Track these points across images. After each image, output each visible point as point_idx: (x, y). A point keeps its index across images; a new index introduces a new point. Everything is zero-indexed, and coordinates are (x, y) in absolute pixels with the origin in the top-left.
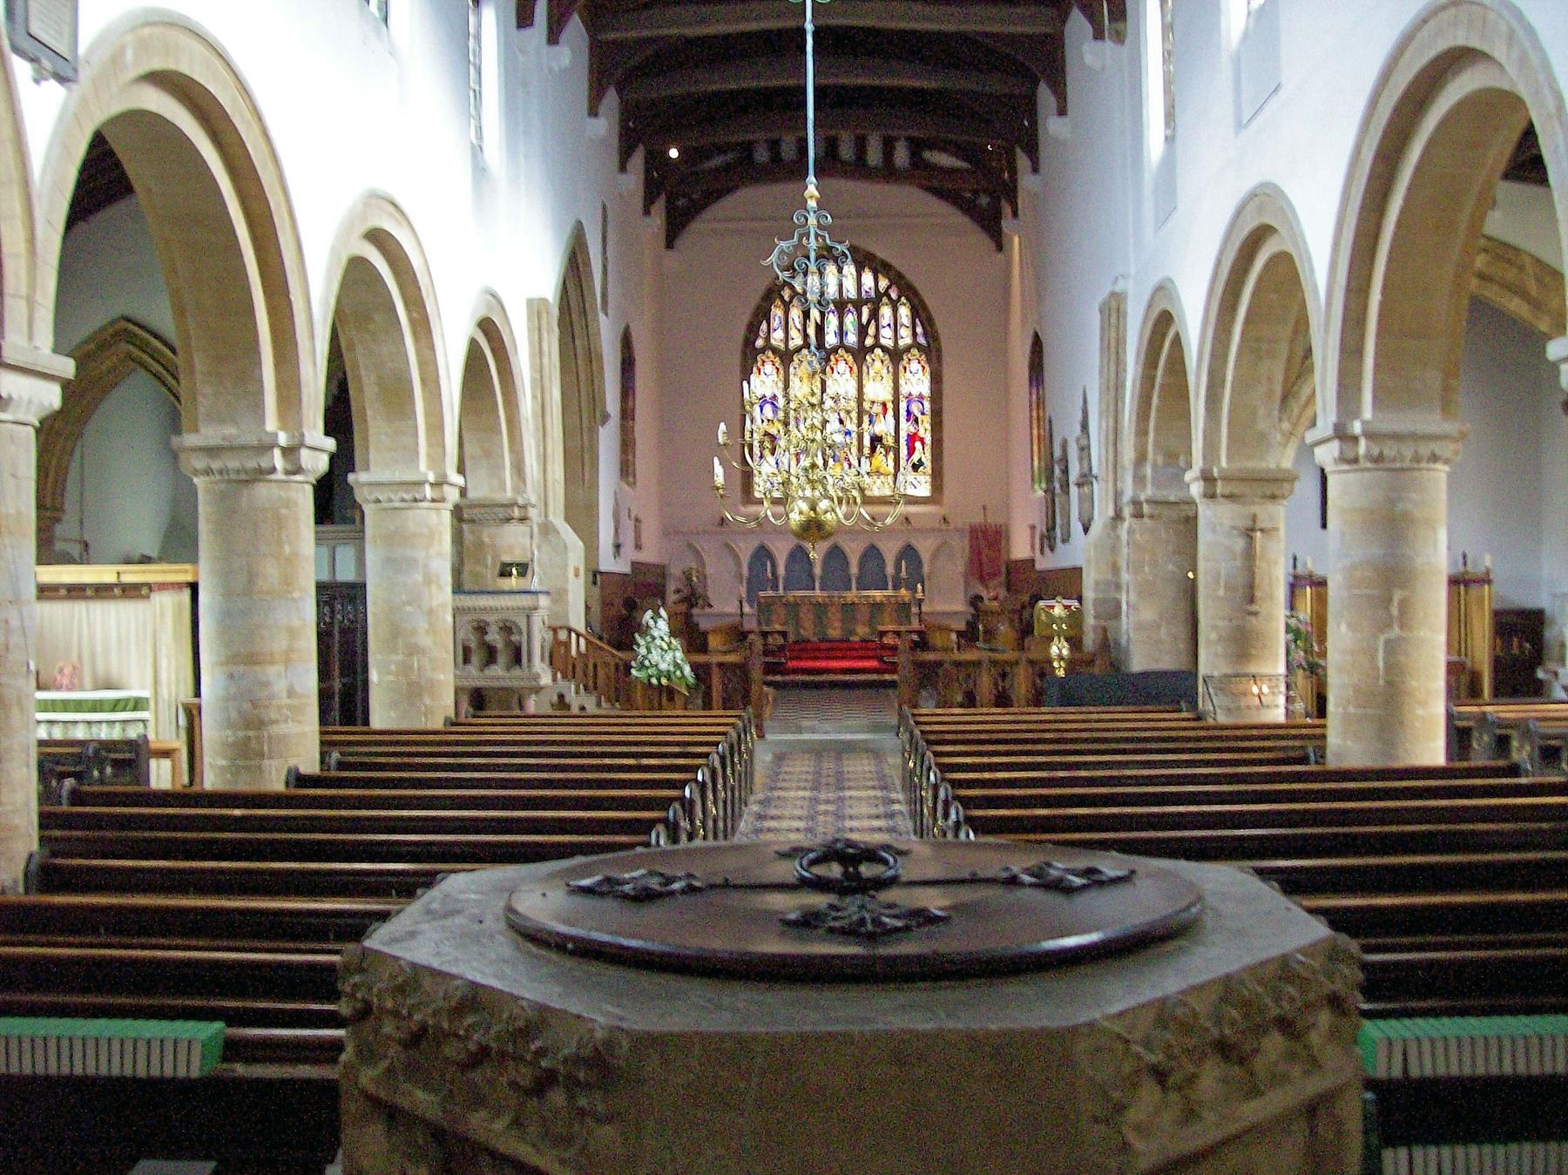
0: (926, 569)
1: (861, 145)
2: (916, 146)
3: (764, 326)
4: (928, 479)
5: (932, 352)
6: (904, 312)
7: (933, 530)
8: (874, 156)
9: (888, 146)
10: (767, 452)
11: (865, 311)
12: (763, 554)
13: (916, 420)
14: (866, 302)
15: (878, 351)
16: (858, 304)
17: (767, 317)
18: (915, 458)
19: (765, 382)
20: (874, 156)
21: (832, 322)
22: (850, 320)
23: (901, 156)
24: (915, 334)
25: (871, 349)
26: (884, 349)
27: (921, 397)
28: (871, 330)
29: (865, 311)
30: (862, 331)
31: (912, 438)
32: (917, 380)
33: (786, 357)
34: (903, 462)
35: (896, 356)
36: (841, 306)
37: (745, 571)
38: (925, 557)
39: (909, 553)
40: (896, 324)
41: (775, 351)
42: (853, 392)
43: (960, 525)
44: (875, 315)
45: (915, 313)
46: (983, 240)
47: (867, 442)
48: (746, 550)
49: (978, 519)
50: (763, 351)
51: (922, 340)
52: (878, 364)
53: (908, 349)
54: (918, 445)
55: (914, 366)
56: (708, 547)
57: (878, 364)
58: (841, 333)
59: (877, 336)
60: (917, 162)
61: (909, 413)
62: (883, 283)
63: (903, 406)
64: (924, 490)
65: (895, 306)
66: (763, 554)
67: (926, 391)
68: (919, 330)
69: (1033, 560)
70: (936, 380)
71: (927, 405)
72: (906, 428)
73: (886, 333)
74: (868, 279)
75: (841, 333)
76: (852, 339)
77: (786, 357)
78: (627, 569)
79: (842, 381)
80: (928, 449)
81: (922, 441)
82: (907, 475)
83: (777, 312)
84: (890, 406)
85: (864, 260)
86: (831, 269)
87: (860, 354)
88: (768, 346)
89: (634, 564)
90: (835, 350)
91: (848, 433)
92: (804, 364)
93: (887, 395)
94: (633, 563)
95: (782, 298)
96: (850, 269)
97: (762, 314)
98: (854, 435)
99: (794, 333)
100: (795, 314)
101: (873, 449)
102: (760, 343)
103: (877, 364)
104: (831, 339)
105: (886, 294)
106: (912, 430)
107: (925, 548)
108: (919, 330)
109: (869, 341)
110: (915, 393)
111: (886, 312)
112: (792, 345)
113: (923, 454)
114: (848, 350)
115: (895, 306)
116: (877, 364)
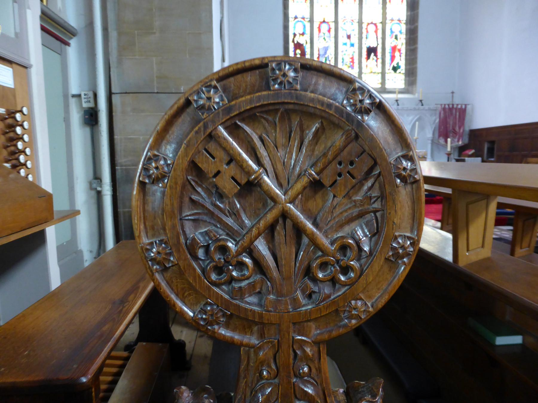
4: (403, 77)
7: (415, 109)
13: (396, 38)
18: (394, 64)
31: (394, 49)
43: (432, 106)
49: (447, 101)
54: (397, 54)
61: (392, 32)
67: (404, 18)
72: (390, 43)
80: (403, 56)
81: (399, 50)
82: (390, 74)
84: (380, 26)
91: (352, 45)
101: (368, 57)
110: (396, 18)
113: (401, 60)
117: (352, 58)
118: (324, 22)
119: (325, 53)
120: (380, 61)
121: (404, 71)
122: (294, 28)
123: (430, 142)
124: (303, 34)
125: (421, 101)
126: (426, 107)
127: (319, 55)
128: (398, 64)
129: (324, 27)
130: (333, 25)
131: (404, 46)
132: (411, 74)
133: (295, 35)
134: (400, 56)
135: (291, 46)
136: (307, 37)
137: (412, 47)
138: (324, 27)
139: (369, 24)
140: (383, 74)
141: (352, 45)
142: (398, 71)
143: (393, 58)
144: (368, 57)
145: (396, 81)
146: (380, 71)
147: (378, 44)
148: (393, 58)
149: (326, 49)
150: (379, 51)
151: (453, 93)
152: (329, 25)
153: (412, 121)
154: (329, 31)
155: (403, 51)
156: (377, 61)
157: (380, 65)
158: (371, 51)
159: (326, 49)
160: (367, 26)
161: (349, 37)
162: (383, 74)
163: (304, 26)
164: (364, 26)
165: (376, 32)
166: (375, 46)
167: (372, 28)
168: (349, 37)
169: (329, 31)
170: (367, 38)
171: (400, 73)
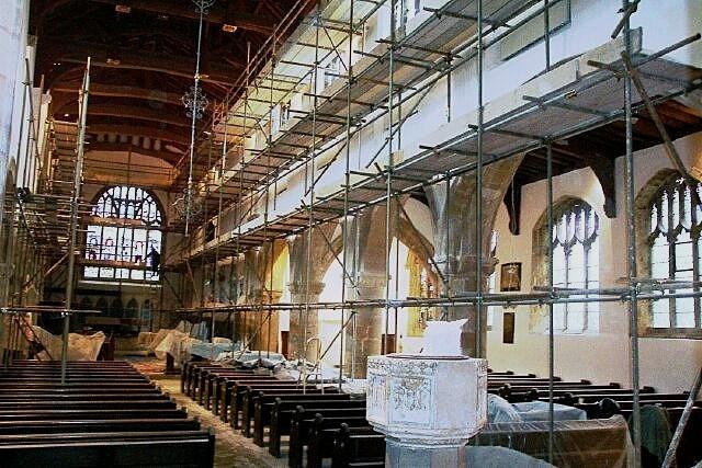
1: (141, 140)
2: (163, 144)
6: (153, 207)
8: (146, 144)
9: (152, 142)
16: (135, 202)
20: (146, 144)
22: (131, 210)
23: (157, 146)
44: (141, 207)
51: (159, 219)
60: (163, 148)
62: (146, 195)
63: (150, 244)
65: (150, 203)
83: (101, 200)
111: (145, 207)
115: (150, 203)
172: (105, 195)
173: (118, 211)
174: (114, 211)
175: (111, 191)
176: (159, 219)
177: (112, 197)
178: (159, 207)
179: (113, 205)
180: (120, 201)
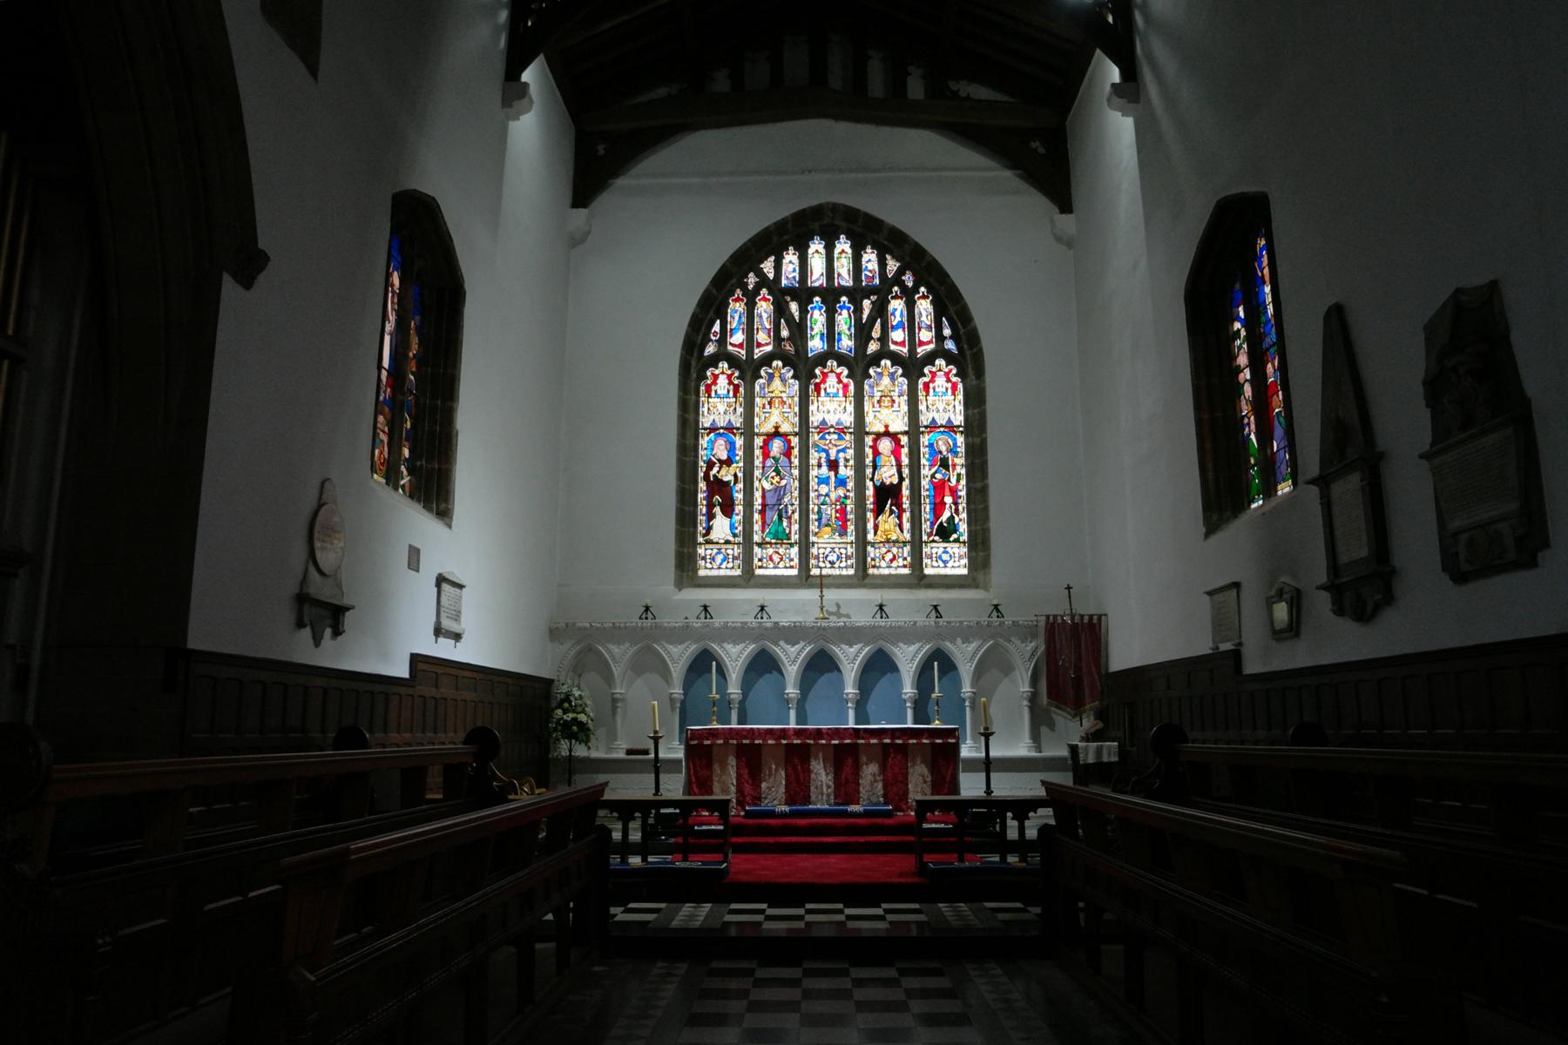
0: (967, 689)
3: (717, 327)
5: (968, 360)
6: (924, 307)
8: (877, 85)
10: (717, 510)
11: (867, 304)
12: (703, 663)
13: (944, 464)
14: (867, 292)
15: (886, 363)
16: (856, 294)
17: (722, 315)
19: (719, 405)
21: (818, 318)
22: (844, 320)
23: (916, 89)
24: (940, 338)
25: (876, 360)
26: (896, 359)
27: (950, 428)
28: (876, 332)
29: (867, 304)
30: (862, 333)
31: (939, 488)
32: (944, 402)
33: (748, 370)
34: (926, 527)
35: (912, 367)
36: (830, 295)
37: (678, 691)
38: (966, 671)
39: (938, 663)
40: (915, 321)
41: (733, 361)
42: (848, 419)
44: (881, 310)
45: (940, 311)
46: (1035, 203)
47: (870, 492)
48: (678, 656)
50: (714, 361)
51: (950, 345)
52: (886, 380)
53: (930, 359)
54: (948, 500)
55: (940, 381)
56: (619, 654)
57: (886, 380)
58: (831, 334)
59: (884, 339)
62: (892, 266)
63: (925, 440)
64: (959, 567)
66: (703, 663)
67: (959, 419)
68: (947, 332)
69: (1236, 655)
70: (975, 400)
71: (960, 439)
73: (898, 335)
74: (870, 259)
75: (831, 334)
76: (846, 344)
77: (748, 370)
78: (402, 671)
79: (831, 407)
81: (954, 492)
83: (736, 309)
85: (867, 231)
86: (816, 247)
87: (859, 366)
88: (723, 355)
89: (416, 659)
90: (821, 359)
91: (842, 483)
92: (781, 386)
93: (899, 424)
94: (416, 659)
95: (744, 286)
96: (843, 246)
97: (711, 307)
98: (851, 485)
99: (761, 337)
100: (764, 308)
102: (710, 349)
103: (886, 381)
104: (816, 345)
105: (897, 279)
106: (938, 476)
107: (965, 656)
108: (947, 332)
109: (873, 347)
111: (897, 306)
112: (758, 353)
114: (842, 360)
116: (886, 381)
117: (843, 512)
118: (777, 433)
119: (780, 500)
120: (906, 516)
121: (965, 538)
122: (712, 448)
123: (1026, 703)
124: (728, 462)
125: (996, 607)
126: (1008, 620)
127: (764, 505)
128: (952, 518)
129: (777, 446)
130: (795, 441)
131: (963, 482)
132: (979, 545)
133: (710, 465)
134: (956, 504)
135: (702, 485)
136: (738, 467)
137: (979, 485)
138: (777, 446)
139: (878, 436)
140: (917, 545)
141: (842, 483)
142: (955, 536)
143: (938, 508)
144: (879, 511)
145: (949, 559)
146: (907, 536)
147: (901, 479)
148: (938, 508)
149: (780, 492)
150: (905, 492)
151: (1069, 588)
152: (789, 442)
153: (975, 653)
154: (788, 453)
155: (963, 493)
156: (900, 517)
157: (907, 526)
158: (887, 495)
159: (780, 492)
160: (875, 441)
161: (833, 465)
162: (917, 545)
163: (731, 447)
164: (869, 440)
165: (896, 453)
166: (895, 480)
167: (885, 445)
168: (833, 465)
169: (788, 453)
170: (875, 467)
171: (956, 541)
172: (752, 280)
173: (800, 331)
174: (785, 333)
175: (768, 267)
176: (950, 345)
177: (774, 286)
178: (950, 305)
179: (780, 311)
180: (804, 294)
